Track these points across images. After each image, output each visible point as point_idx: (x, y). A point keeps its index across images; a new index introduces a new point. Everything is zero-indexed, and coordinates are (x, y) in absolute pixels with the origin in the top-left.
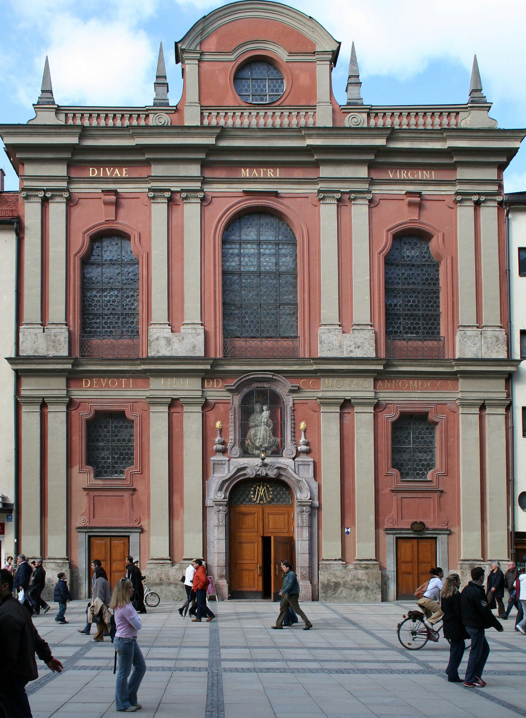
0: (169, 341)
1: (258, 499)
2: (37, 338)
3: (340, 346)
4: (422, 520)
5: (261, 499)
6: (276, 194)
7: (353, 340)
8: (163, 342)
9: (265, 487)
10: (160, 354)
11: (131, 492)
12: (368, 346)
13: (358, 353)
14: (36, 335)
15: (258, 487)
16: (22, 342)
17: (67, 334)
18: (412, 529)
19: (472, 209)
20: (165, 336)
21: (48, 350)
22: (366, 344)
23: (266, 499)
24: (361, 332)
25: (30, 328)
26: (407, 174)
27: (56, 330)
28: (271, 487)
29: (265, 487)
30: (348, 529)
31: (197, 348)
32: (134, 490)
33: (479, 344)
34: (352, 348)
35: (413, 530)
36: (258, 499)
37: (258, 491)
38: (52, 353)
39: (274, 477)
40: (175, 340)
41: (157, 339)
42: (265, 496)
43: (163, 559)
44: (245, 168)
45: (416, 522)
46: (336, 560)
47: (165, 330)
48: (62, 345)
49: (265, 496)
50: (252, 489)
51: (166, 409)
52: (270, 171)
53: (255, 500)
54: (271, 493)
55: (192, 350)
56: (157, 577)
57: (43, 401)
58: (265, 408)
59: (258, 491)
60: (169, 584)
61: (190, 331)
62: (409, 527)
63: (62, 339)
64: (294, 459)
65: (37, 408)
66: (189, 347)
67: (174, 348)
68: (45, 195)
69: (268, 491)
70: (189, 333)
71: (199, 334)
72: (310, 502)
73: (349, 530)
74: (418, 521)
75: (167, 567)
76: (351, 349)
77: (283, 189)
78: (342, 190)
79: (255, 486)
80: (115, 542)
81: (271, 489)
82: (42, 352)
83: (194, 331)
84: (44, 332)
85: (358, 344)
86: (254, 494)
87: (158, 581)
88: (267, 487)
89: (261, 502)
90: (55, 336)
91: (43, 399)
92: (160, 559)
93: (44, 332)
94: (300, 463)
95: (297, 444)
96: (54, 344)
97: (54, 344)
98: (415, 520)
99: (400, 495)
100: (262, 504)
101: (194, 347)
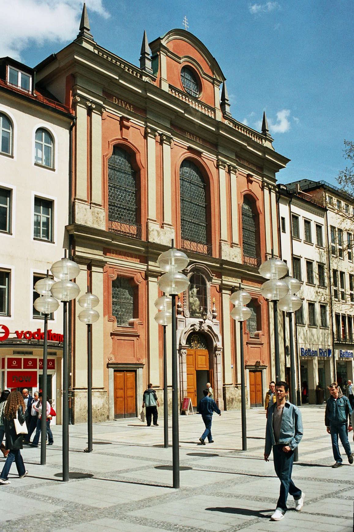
2: (87, 212)
3: (229, 255)
8: (155, 233)
11: (138, 338)
14: (86, 210)
16: (77, 213)
21: (93, 223)
22: (238, 256)
25: (82, 203)
32: (138, 336)
38: (96, 226)
40: (161, 233)
41: (153, 230)
46: (230, 385)
48: (102, 222)
57: (90, 263)
63: (102, 217)
65: (85, 267)
68: (91, 105)
71: (172, 232)
77: (205, 154)
78: (227, 163)
80: (129, 374)
82: (90, 224)
83: (170, 229)
84: (90, 208)
85: (236, 255)
90: (98, 214)
91: (91, 261)
93: (90, 208)
94: (215, 323)
96: (97, 219)
97: (97, 219)
99: (250, 346)
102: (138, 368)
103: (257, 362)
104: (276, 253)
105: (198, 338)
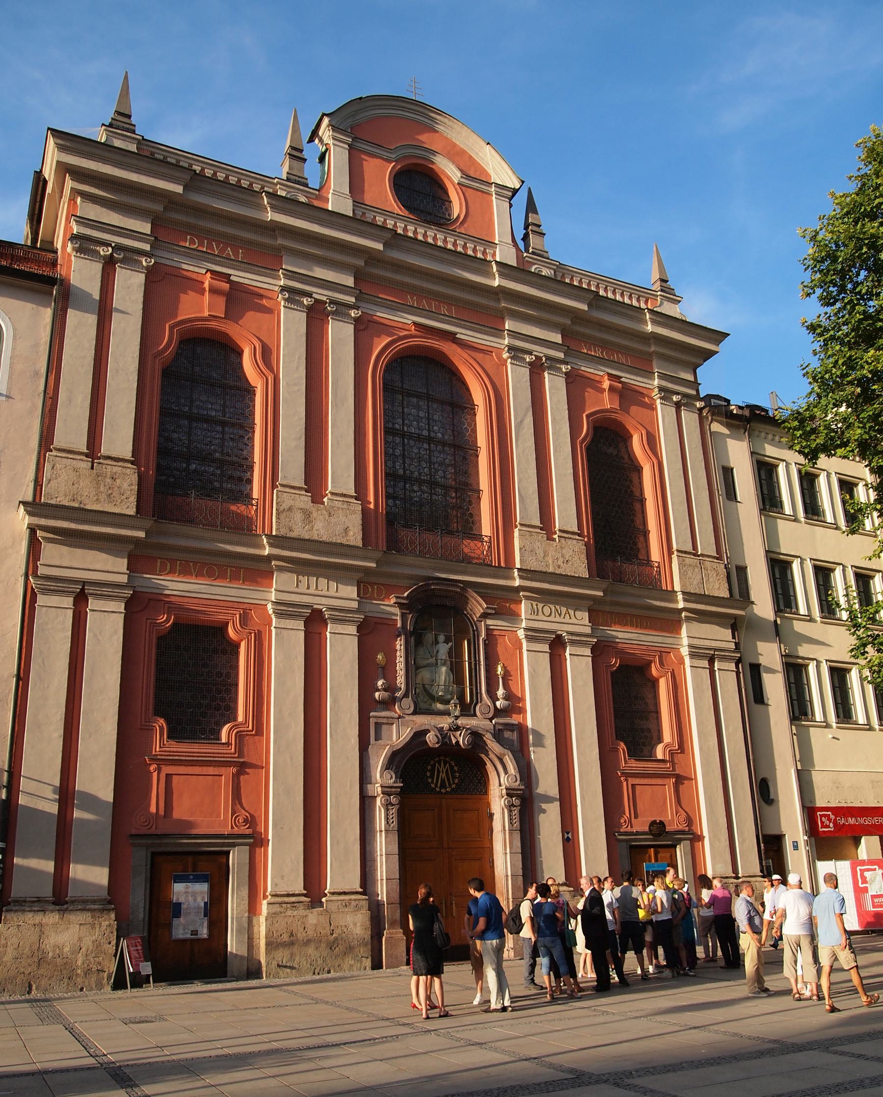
0: (307, 515)
1: (439, 786)
4: (662, 819)
5: (443, 786)
6: (451, 337)
7: (560, 550)
8: (298, 516)
9: (448, 765)
10: (293, 535)
12: (578, 562)
13: (568, 570)
15: (437, 765)
17: (135, 478)
18: (650, 832)
19: (674, 409)
20: (302, 507)
23: (450, 785)
24: (570, 542)
26: (602, 353)
27: (115, 469)
28: (456, 765)
29: (448, 765)
30: (568, 833)
31: (351, 533)
33: (699, 577)
34: (560, 562)
35: (652, 834)
36: (439, 786)
37: (439, 771)
39: (437, 746)
41: (290, 509)
42: (449, 780)
43: (293, 895)
44: (412, 295)
45: (655, 821)
47: (302, 498)
49: (449, 780)
50: (429, 767)
51: (300, 625)
52: (444, 307)
53: (433, 786)
54: (457, 774)
55: (344, 534)
56: (285, 931)
58: (441, 638)
59: (439, 771)
60: (308, 942)
61: (340, 505)
62: (647, 829)
64: (491, 720)
66: (339, 529)
67: (316, 527)
69: (453, 772)
70: (339, 508)
71: (354, 512)
72: (520, 790)
73: (570, 835)
74: (658, 820)
75: (301, 912)
76: (559, 563)
79: (432, 762)
81: (456, 768)
83: (345, 506)
86: (432, 777)
87: (285, 938)
88: (450, 764)
89: (443, 791)
92: (288, 895)
95: (494, 698)
98: (653, 819)
100: (445, 793)
101: (346, 530)
102: (234, 845)
103: (653, 823)
104: (706, 544)
105: (452, 767)
